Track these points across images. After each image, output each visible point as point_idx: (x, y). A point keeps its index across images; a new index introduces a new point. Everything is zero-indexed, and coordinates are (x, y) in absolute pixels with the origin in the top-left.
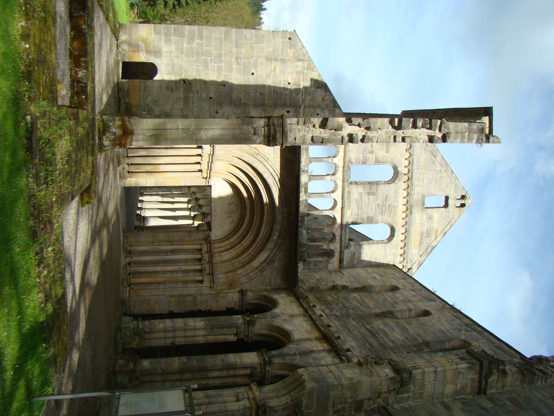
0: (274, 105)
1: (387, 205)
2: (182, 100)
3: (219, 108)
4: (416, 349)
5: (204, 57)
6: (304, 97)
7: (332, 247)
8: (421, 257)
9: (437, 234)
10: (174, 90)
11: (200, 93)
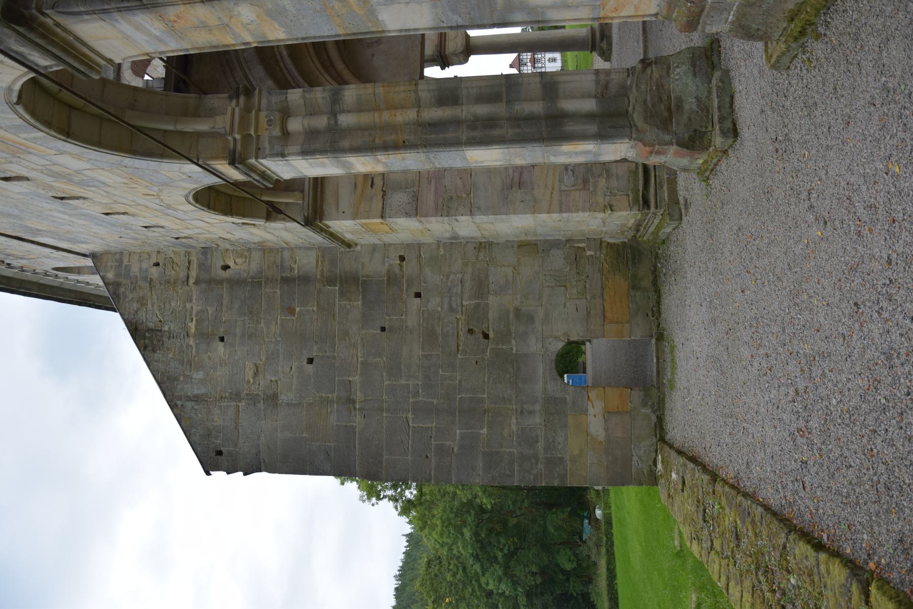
0: (260, 284)
2: (492, 287)
3: (397, 270)
5: (435, 401)
6: (188, 306)
10: (512, 316)
11: (446, 306)
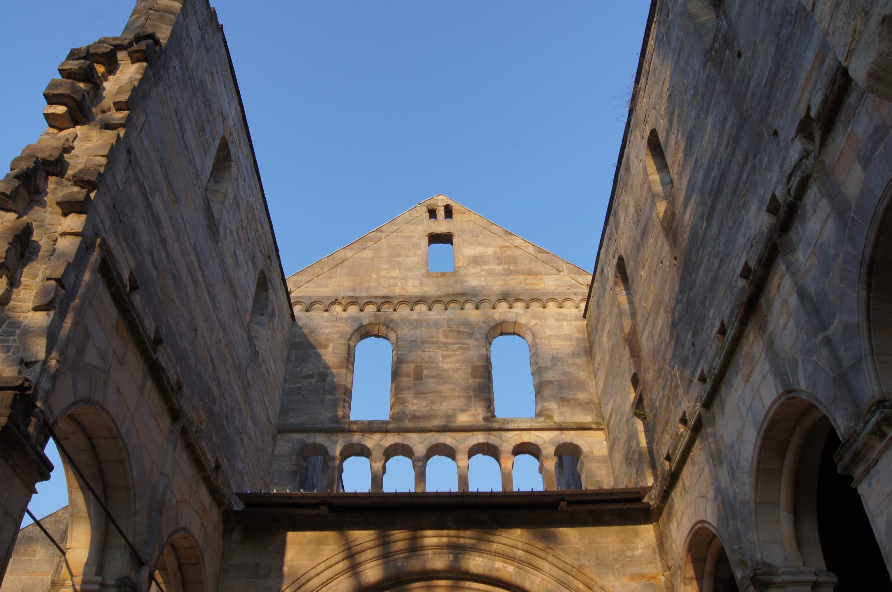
1: (445, 340)
4: (728, 52)
7: (549, 451)
8: (561, 269)
9: (510, 247)
